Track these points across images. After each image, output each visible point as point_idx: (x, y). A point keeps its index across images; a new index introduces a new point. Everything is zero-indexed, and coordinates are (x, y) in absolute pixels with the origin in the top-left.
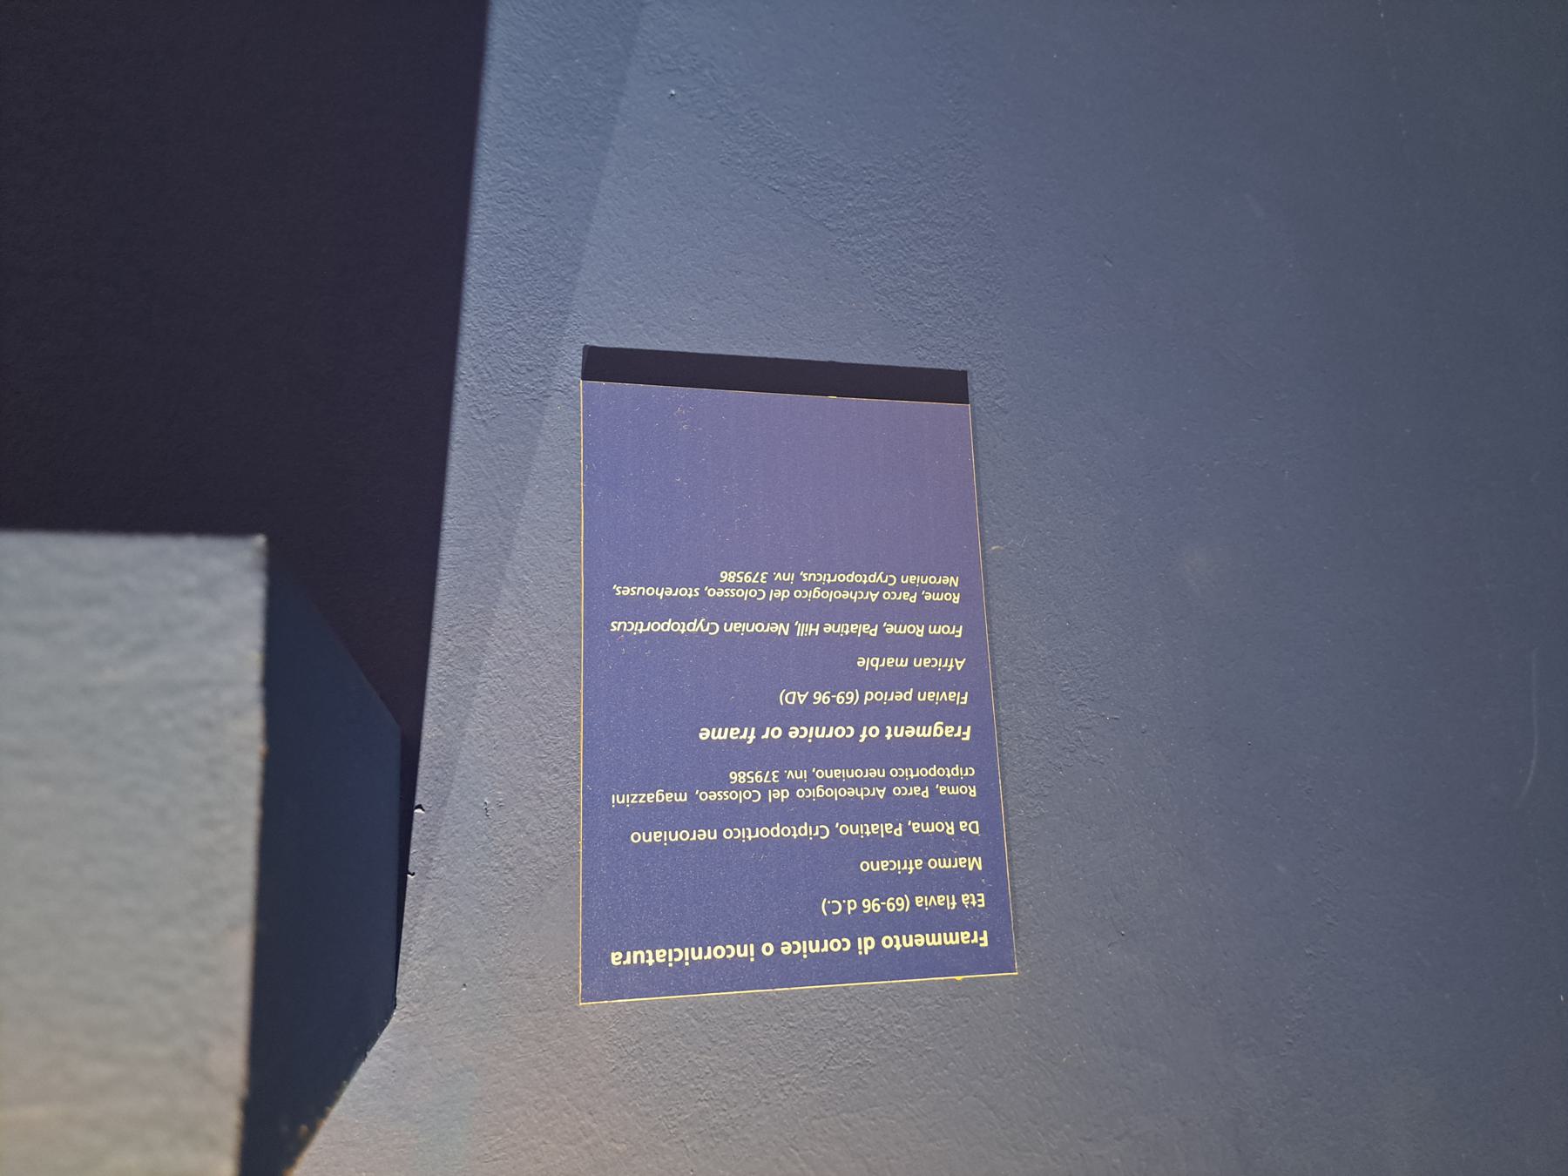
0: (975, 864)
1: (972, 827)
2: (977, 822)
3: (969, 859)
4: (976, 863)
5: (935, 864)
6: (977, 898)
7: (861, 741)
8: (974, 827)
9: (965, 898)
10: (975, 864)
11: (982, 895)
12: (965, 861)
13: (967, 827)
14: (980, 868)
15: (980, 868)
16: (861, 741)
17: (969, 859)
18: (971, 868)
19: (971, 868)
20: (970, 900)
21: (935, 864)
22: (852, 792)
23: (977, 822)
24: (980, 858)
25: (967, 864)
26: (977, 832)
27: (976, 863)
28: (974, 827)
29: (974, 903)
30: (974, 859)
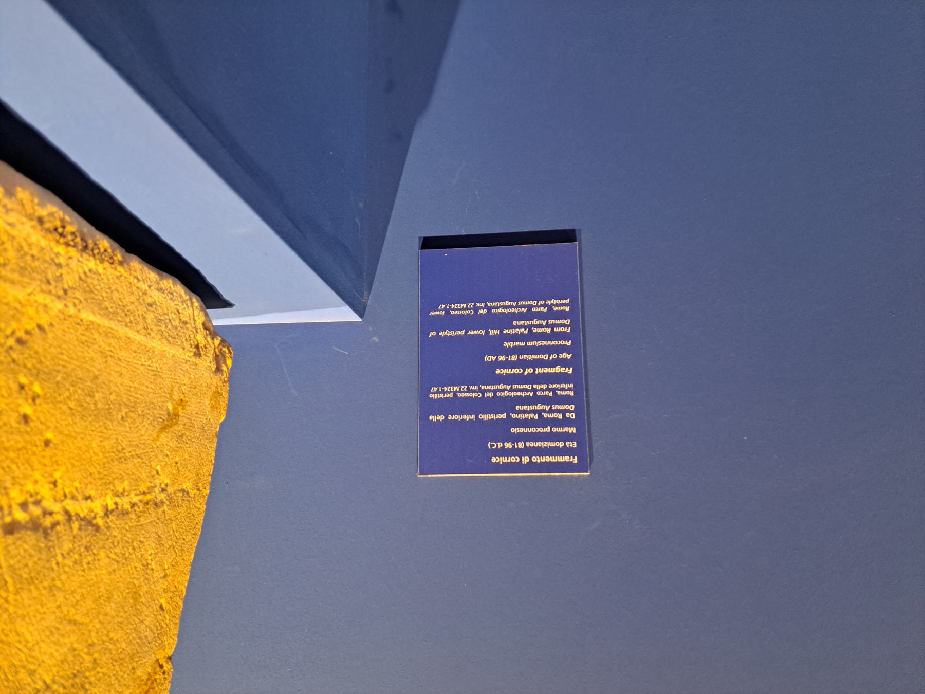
4: (573, 430)
5: (555, 430)
6: (573, 443)
8: (572, 416)
9: (567, 443)
11: (575, 442)
14: (575, 432)
15: (575, 432)
18: (571, 432)
19: (571, 432)
20: (570, 444)
21: (555, 430)
22: (519, 394)
26: (574, 417)
27: (573, 430)
28: (572, 416)
29: (571, 445)
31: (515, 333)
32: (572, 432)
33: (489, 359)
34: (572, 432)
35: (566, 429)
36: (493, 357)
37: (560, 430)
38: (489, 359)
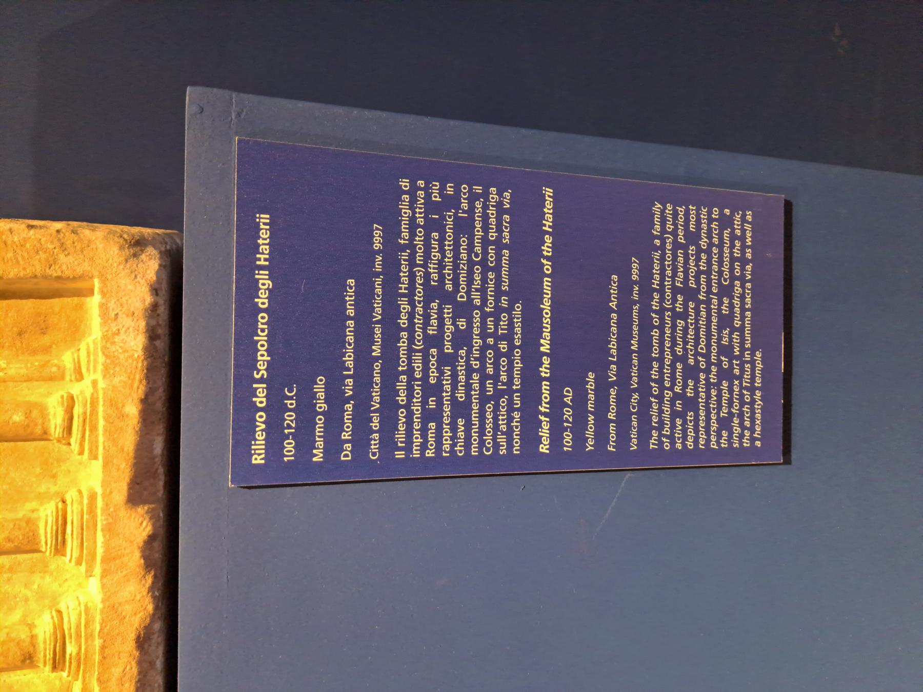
0: (319, 455)
2: (350, 458)
3: (322, 450)
8: (346, 456)
10: (319, 455)
12: (320, 447)
13: (346, 450)
14: (315, 459)
15: (315, 459)
17: (322, 450)
18: (315, 451)
19: (315, 451)
24: (322, 460)
25: (318, 448)
26: (342, 459)
28: (346, 456)
30: (322, 455)
32: (316, 455)
34: (316, 455)
35: (320, 443)
37: (319, 430)
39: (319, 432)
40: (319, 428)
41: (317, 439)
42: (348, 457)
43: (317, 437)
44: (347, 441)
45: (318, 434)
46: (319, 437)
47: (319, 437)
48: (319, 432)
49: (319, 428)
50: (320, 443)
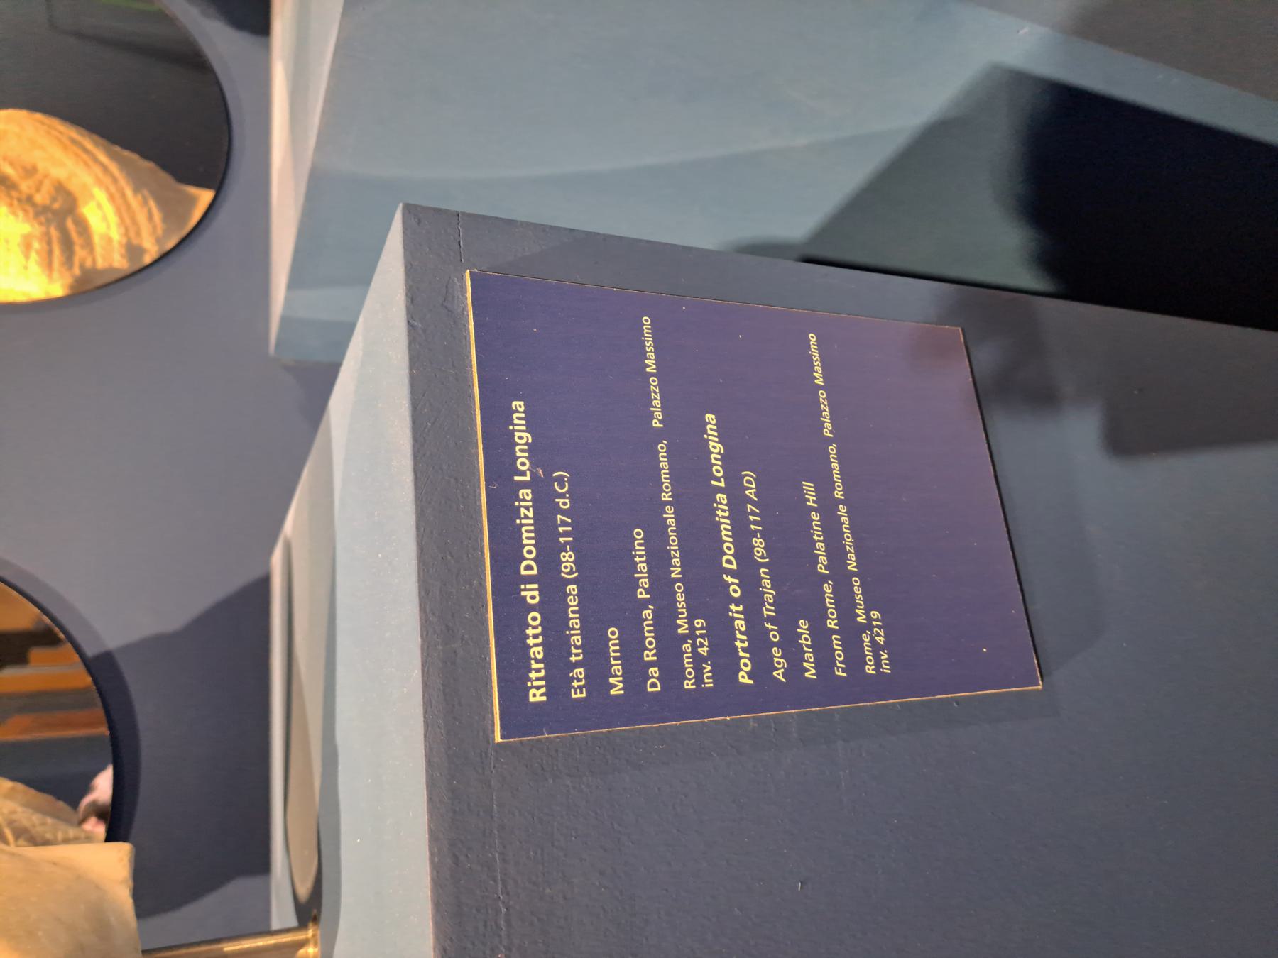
0: (617, 686)
1: (654, 684)
2: (658, 689)
3: (621, 679)
7: (724, 576)
8: (653, 685)
13: (653, 677)
16: (724, 576)
17: (621, 679)
18: (612, 680)
19: (612, 680)
23: (658, 689)
25: (616, 676)
26: (649, 690)
28: (653, 685)
31: (815, 542)
33: (749, 482)
35: (617, 668)
36: (753, 491)
37: (613, 649)
38: (749, 482)
39: (614, 651)
40: (614, 645)
41: (613, 662)
42: (657, 687)
43: (611, 659)
44: (652, 664)
45: (612, 654)
46: (615, 658)
47: (615, 658)
48: (614, 651)
49: (614, 645)
50: (617, 668)
